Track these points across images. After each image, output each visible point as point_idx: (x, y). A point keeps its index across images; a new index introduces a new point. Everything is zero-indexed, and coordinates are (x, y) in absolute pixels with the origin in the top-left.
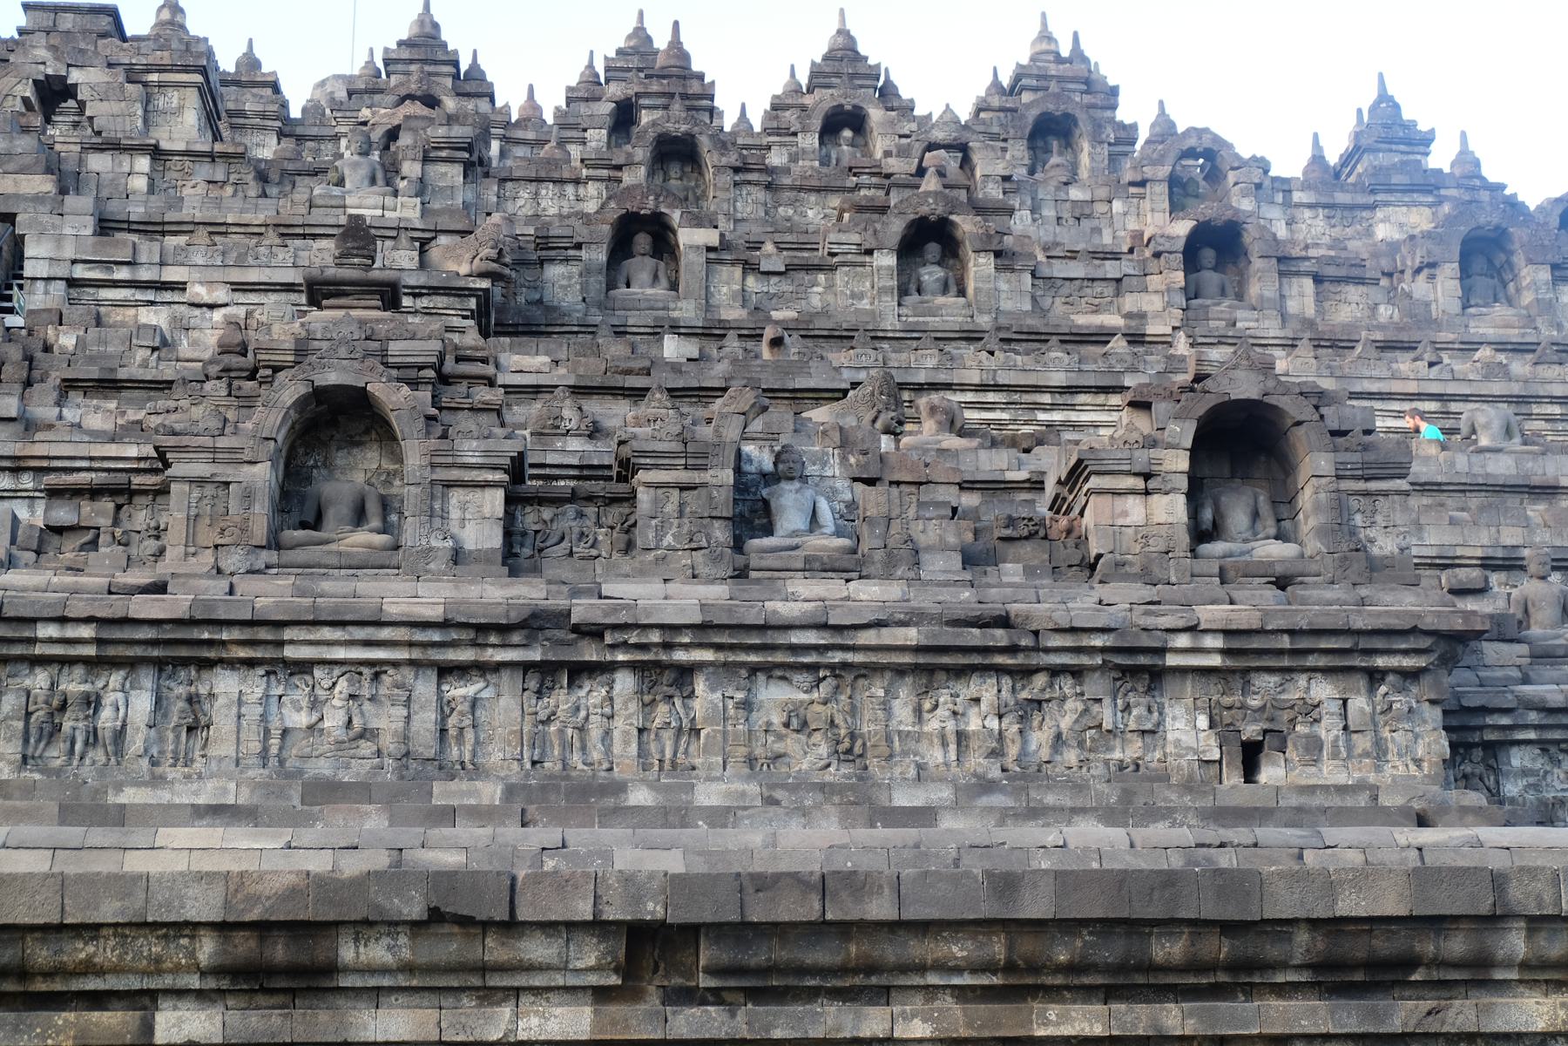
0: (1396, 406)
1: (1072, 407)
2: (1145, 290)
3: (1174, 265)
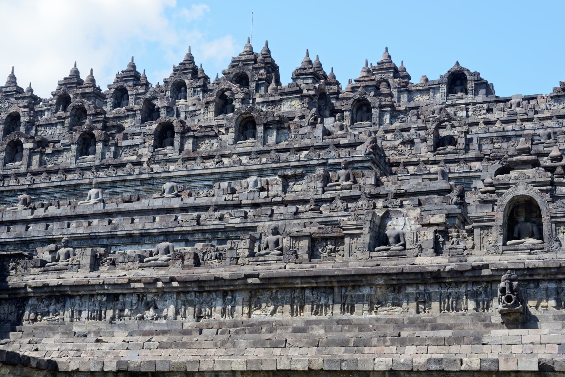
0: (207, 177)
1: (116, 187)
2: (145, 147)
3: (151, 138)
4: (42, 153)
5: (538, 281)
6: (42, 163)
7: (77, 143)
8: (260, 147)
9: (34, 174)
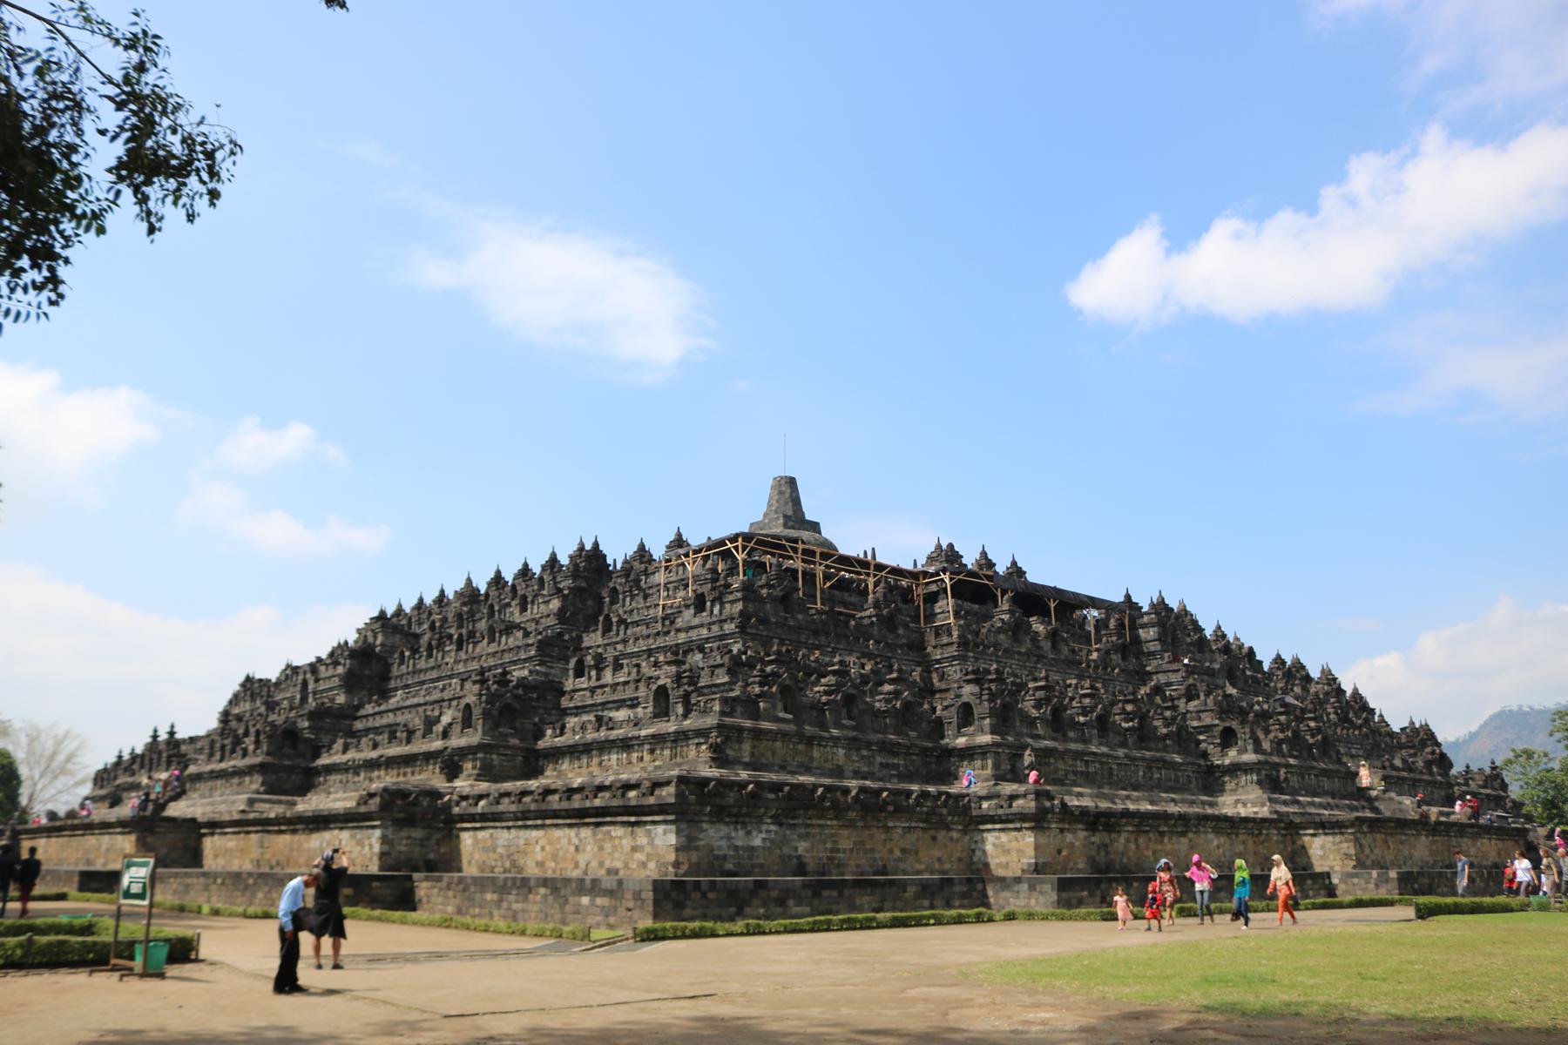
4: (414, 658)
5: (467, 754)
6: (414, 665)
7: (427, 651)
8: (497, 649)
9: (408, 673)
